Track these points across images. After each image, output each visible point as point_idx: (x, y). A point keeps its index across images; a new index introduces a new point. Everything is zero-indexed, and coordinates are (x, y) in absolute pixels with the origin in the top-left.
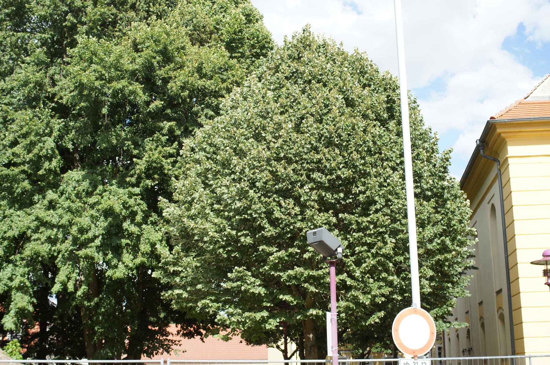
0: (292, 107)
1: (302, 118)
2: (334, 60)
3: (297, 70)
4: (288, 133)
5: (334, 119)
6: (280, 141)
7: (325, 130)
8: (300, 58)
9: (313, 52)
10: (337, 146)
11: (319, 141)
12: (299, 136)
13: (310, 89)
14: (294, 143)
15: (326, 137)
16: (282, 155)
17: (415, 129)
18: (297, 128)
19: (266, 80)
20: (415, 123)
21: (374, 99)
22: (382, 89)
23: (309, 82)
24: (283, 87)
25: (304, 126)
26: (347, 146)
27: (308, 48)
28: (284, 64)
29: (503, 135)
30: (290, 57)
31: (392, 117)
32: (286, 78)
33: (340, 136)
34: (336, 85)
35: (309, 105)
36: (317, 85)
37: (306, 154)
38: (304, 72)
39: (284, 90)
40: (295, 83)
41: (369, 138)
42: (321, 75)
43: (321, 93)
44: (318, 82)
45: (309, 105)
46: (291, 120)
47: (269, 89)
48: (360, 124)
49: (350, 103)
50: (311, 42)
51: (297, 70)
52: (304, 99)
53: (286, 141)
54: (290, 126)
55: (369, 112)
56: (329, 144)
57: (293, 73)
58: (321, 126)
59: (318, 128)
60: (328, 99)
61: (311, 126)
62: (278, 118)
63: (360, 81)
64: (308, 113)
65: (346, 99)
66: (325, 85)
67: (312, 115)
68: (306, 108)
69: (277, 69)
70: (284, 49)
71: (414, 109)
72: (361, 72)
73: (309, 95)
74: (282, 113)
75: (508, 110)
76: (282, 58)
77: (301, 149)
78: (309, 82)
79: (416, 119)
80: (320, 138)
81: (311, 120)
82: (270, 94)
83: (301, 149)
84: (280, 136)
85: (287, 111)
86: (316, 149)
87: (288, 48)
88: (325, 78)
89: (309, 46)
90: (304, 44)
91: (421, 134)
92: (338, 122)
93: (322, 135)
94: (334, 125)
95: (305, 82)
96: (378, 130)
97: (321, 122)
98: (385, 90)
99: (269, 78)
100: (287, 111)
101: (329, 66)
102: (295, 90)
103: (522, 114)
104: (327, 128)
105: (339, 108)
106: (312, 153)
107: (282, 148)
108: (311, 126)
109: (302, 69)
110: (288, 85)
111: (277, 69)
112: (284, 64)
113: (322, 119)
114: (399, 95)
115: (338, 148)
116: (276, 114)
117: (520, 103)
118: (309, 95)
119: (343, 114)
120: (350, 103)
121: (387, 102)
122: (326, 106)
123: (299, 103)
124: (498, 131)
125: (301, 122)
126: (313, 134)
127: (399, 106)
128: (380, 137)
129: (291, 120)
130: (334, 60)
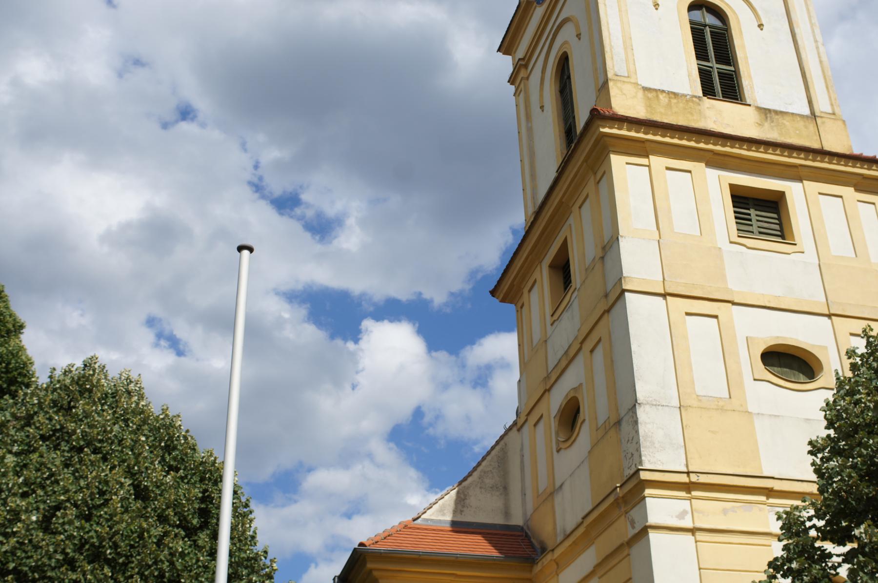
0: (43, 487)
1: (58, 508)
2: (126, 421)
3: (62, 428)
4: (28, 530)
5: (112, 516)
6: (13, 540)
7: (92, 534)
8: (70, 408)
9: (95, 403)
10: (108, 562)
11: (79, 549)
12: (47, 537)
13: (81, 461)
14: (37, 547)
15: (93, 545)
16: (11, 566)
17: (240, 550)
18: (46, 524)
19: (8, 435)
20: (242, 538)
21: (181, 492)
22: (196, 478)
23: (80, 450)
24: (35, 450)
25: (57, 522)
26: (125, 564)
27: (86, 395)
28: (41, 415)
29: (375, 573)
30: (55, 403)
31: (204, 526)
32: (43, 438)
33: (116, 546)
34: (124, 461)
35: (73, 488)
36: (93, 457)
37: (53, 569)
38: (74, 432)
39: (35, 457)
40: (56, 447)
41: (164, 555)
42: (101, 441)
43: (96, 473)
44: (95, 451)
45: (73, 488)
46: (38, 509)
47: (10, 452)
48: (153, 532)
49: (141, 493)
50: (93, 386)
51: (62, 428)
52: (66, 477)
53: (22, 544)
54: (34, 518)
55: (170, 512)
56: (96, 556)
57: (55, 431)
58: (87, 525)
59: (81, 528)
60: (106, 483)
61: (70, 523)
62: (16, 502)
63: (163, 459)
64: (68, 500)
65: (136, 486)
66: (105, 459)
67: (76, 505)
68: (67, 491)
69: (29, 420)
70: (46, 390)
71: (245, 516)
72: (167, 446)
73: (77, 470)
74: (24, 495)
75: (387, 534)
76: (40, 404)
77: (45, 560)
78: (80, 450)
79: (244, 532)
80: (82, 545)
81: (72, 512)
82: (10, 459)
83: (45, 560)
84: (14, 534)
85: (34, 492)
86: (71, 564)
87: (55, 390)
88: (106, 447)
89: (90, 391)
90: (82, 385)
91: (249, 559)
92: (117, 523)
93: (87, 542)
94: (111, 528)
95: (72, 449)
96: (179, 546)
97: (88, 518)
98: (202, 480)
99: (12, 432)
100: (34, 492)
101: (116, 428)
102: (55, 458)
103: (407, 545)
104: (97, 530)
105: (122, 500)
106: (63, 569)
107: (13, 553)
108: (70, 523)
109: (71, 426)
110: (43, 449)
111: (29, 420)
112: (41, 415)
113: (90, 514)
114: (220, 491)
115: (109, 565)
116: (15, 495)
117: (406, 527)
118: (77, 470)
119: (126, 510)
120: (141, 493)
121: (203, 500)
122: (102, 493)
123: (57, 482)
124: (369, 566)
125: (54, 515)
126: (70, 537)
127: (218, 507)
128: (182, 555)
129: (38, 509)
130: (126, 421)
